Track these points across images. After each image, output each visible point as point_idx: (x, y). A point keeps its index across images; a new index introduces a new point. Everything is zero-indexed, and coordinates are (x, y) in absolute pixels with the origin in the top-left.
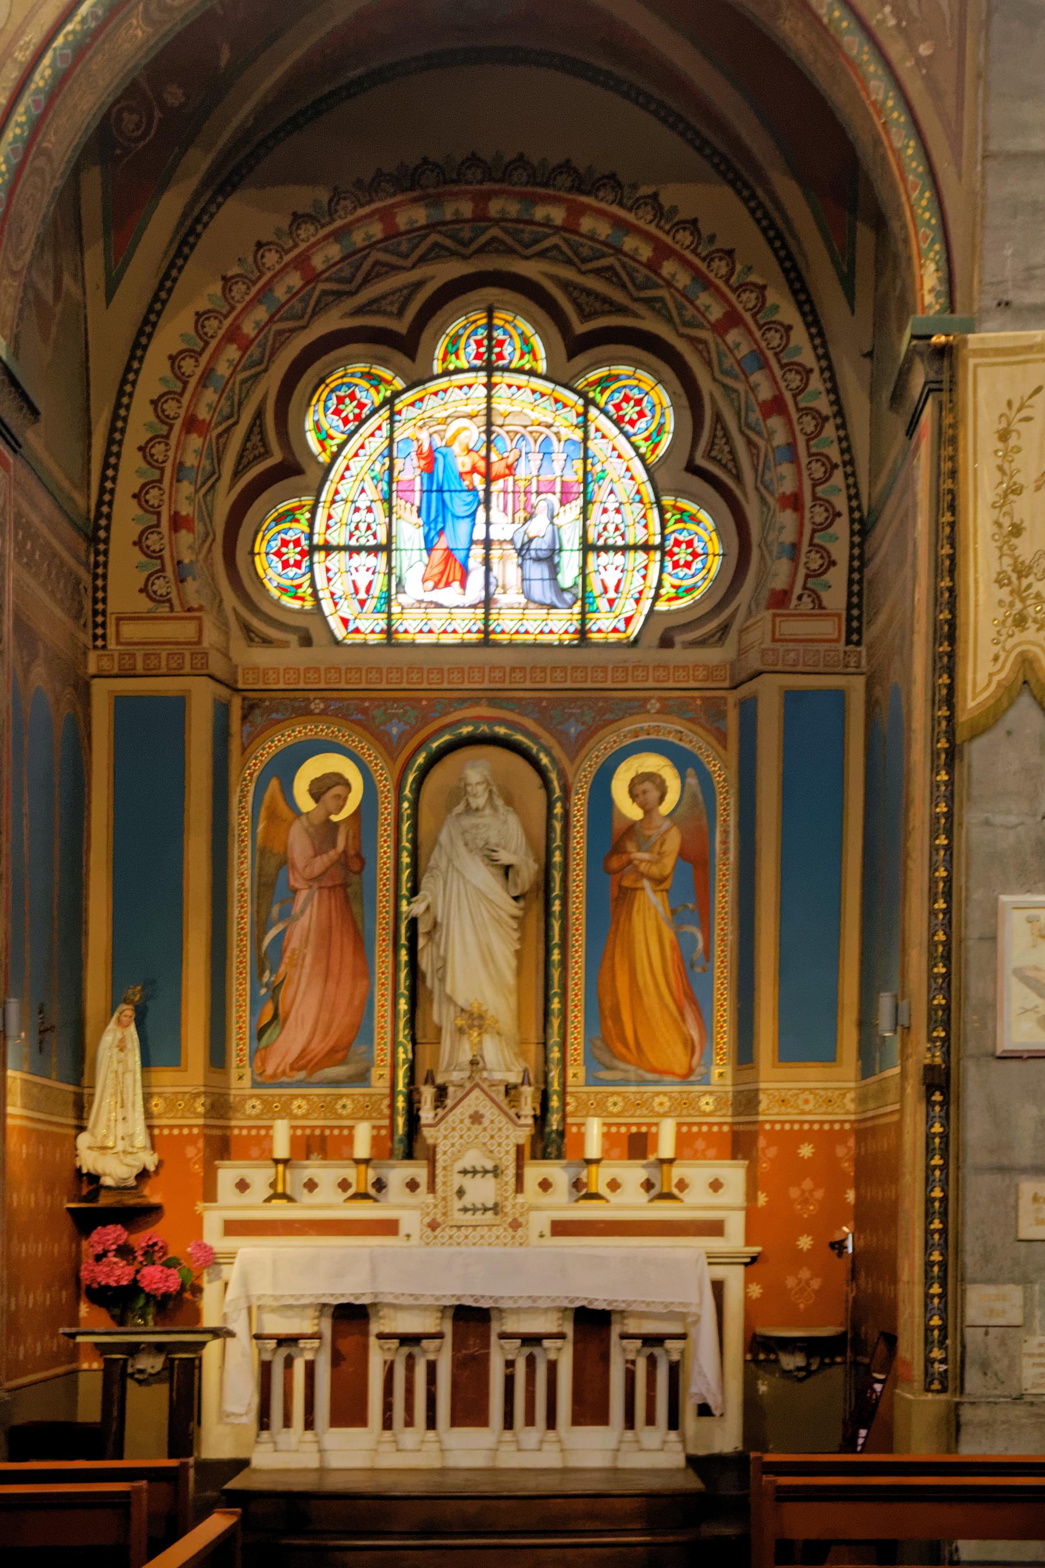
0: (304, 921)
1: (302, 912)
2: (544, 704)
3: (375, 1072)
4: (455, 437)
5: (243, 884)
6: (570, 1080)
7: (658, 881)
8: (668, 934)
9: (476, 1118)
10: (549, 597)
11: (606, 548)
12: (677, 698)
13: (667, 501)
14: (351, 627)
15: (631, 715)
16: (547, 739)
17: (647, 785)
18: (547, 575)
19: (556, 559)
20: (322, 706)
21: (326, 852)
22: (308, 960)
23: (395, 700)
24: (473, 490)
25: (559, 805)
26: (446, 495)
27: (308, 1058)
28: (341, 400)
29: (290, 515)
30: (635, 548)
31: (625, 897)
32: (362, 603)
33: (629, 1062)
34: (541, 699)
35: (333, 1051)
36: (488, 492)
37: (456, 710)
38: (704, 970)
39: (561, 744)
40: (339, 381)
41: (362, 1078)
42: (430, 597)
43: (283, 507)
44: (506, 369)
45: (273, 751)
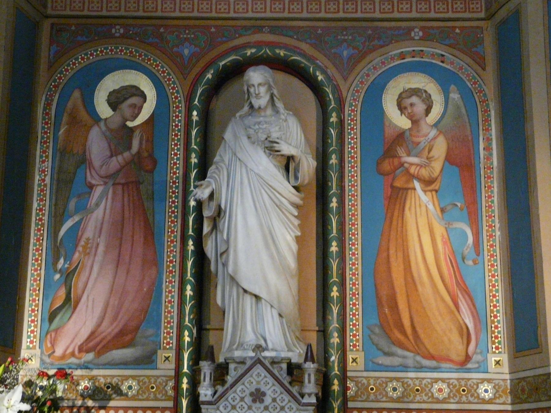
0: (99, 213)
1: (97, 205)
2: (320, 31)
3: (161, 354)
5: (44, 180)
6: (350, 365)
7: (427, 182)
8: (439, 230)
9: (258, 396)
12: (438, 28)
15: (397, 41)
16: (322, 60)
17: (414, 99)
20: (122, 31)
21: (121, 153)
22: (101, 249)
23: (187, 27)
25: (334, 114)
27: (98, 339)
31: (397, 197)
33: (408, 350)
34: (315, 28)
35: (121, 333)
37: (240, 36)
38: (475, 262)
39: (334, 64)
41: (147, 360)
45: (78, 67)
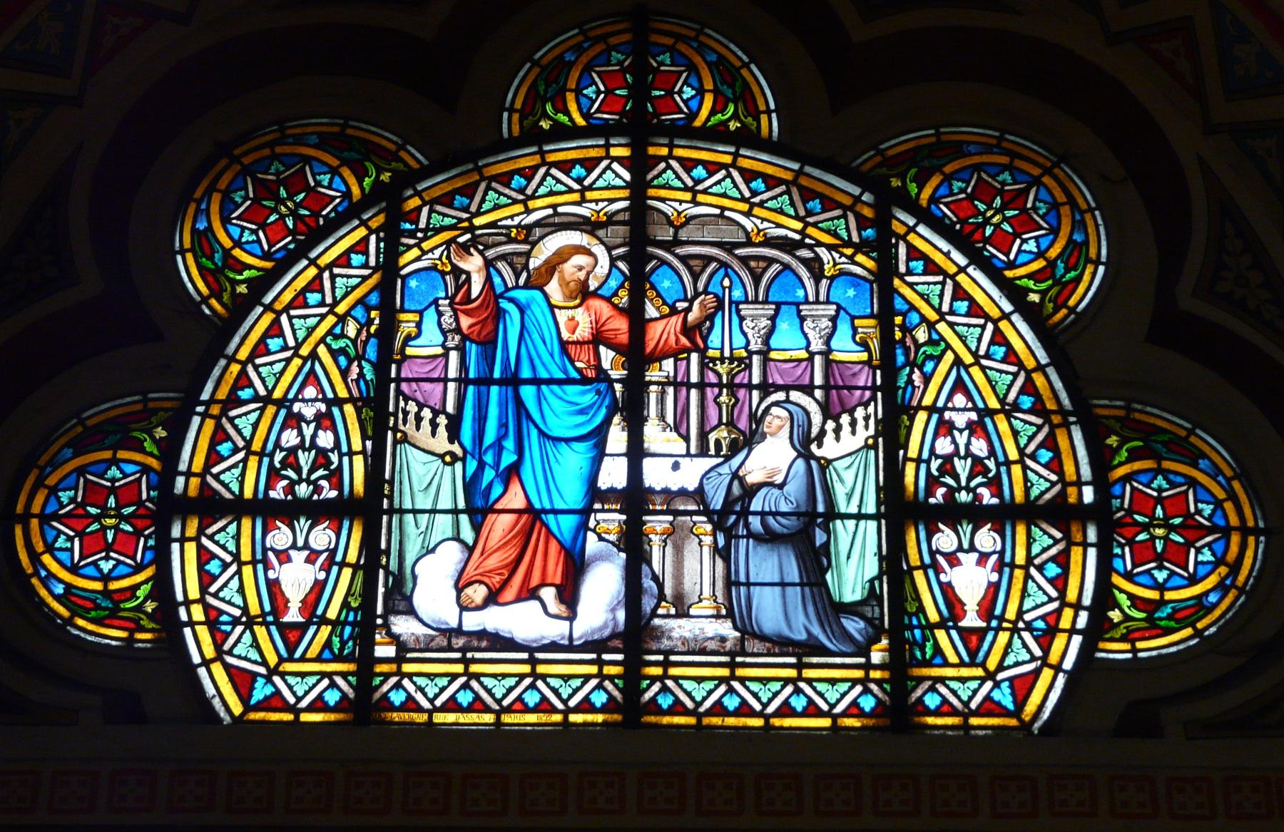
4: (551, 267)
10: (802, 625)
11: (953, 514)
13: (1105, 407)
14: (261, 691)
18: (793, 574)
19: (820, 537)
24: (602, 376)
26: (528, 392)
28: (266, 190)
29: (121, 435)
30: (1030, 512)
32: (292, 635)
36: (636, 387)
40: (267, 152)
42: (472, 622)
43: (96, 414)
44: (686, 131)
